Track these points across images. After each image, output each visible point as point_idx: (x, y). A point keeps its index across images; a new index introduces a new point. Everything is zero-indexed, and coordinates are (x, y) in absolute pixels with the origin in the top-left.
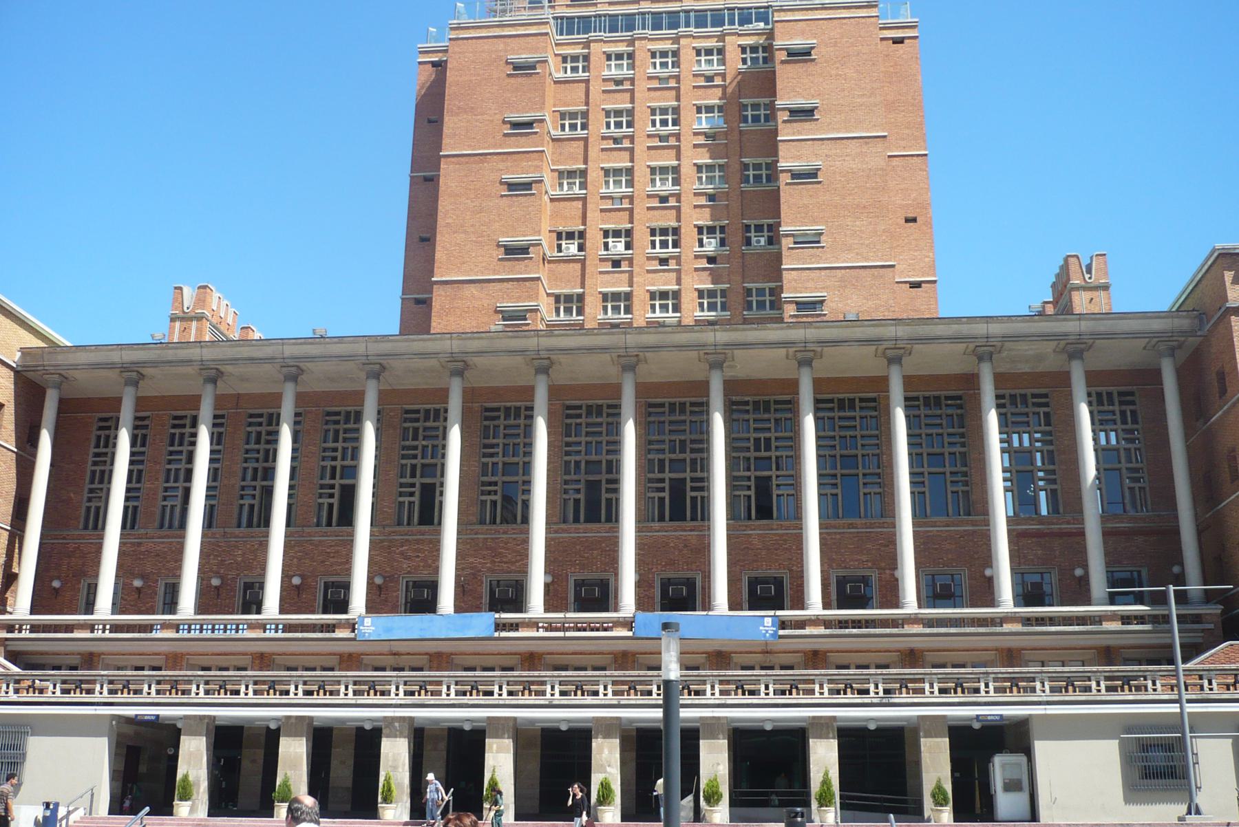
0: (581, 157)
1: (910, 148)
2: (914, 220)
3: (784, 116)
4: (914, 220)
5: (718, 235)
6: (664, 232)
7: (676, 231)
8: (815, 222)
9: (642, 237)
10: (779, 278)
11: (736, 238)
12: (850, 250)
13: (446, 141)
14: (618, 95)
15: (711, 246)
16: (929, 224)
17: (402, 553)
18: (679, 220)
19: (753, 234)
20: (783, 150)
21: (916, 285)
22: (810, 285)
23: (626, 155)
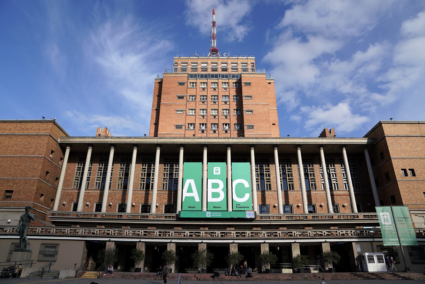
2: (274, 124)
4: (274, 124)
9: (209, 126)
12: (261, 130)
17: (164, 197)
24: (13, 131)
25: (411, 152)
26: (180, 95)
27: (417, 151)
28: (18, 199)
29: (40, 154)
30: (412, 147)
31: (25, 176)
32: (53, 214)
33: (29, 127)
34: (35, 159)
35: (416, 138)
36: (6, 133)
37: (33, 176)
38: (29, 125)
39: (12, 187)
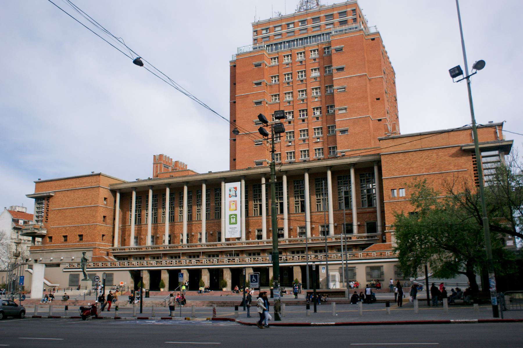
0: (278, 90)
1: (377, 75)
3: (335, 71)
5: (319, 111)
6: (303, 111)
7: (306, 110)
8: (345, 105)
9: (296, 113)
10: (335, 123)
11: (324, 111)
13: (237, 92)
14: (288, 69)
15: (318, 113)
16: (383, 100)
18: (307, 107)
19: (329, 109)
20: (334, 82)
21: (380, 120)
22: (344, 125)
23: (291, 88)
24: (74, 186)
25: (405, 170)
26: (256, 82)
27: (412, 168)
28: (87, 241)
29: (95, 204)
30: (408, 164)
31: (89, 223)
32: (113, 250)
33: (84, 181)
34: (93, 208)
35: (414, 154)
36: (71, 188)
37: (94, 222)
38: (84, 180)
39: (82, 232)
